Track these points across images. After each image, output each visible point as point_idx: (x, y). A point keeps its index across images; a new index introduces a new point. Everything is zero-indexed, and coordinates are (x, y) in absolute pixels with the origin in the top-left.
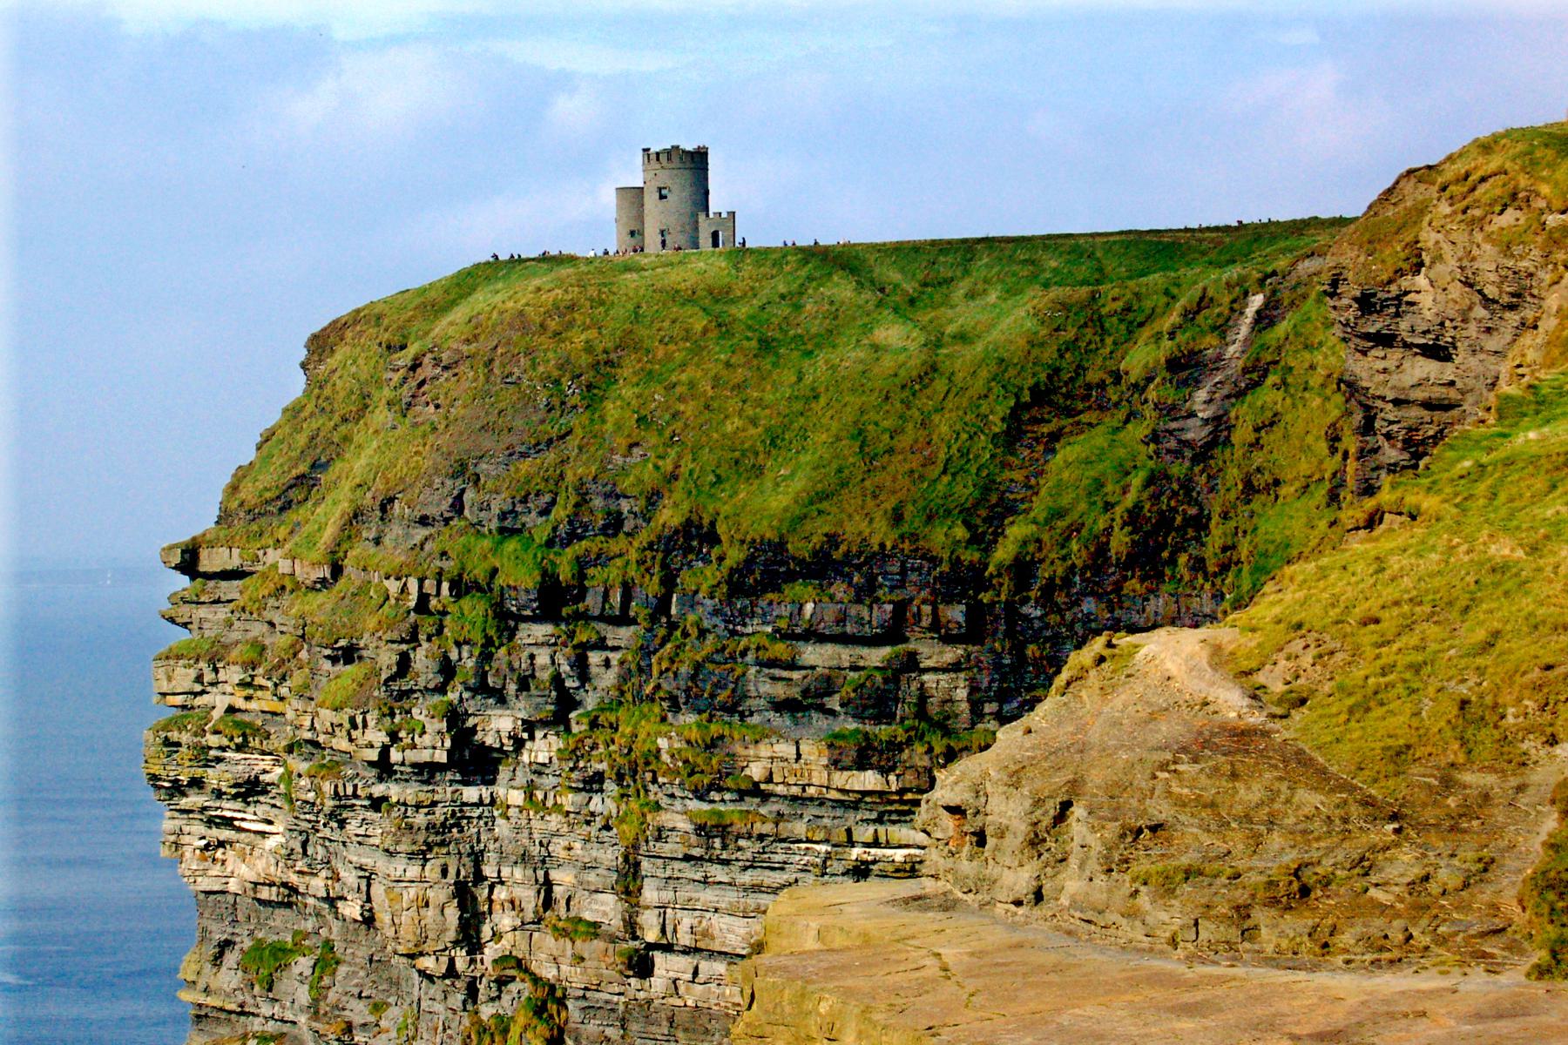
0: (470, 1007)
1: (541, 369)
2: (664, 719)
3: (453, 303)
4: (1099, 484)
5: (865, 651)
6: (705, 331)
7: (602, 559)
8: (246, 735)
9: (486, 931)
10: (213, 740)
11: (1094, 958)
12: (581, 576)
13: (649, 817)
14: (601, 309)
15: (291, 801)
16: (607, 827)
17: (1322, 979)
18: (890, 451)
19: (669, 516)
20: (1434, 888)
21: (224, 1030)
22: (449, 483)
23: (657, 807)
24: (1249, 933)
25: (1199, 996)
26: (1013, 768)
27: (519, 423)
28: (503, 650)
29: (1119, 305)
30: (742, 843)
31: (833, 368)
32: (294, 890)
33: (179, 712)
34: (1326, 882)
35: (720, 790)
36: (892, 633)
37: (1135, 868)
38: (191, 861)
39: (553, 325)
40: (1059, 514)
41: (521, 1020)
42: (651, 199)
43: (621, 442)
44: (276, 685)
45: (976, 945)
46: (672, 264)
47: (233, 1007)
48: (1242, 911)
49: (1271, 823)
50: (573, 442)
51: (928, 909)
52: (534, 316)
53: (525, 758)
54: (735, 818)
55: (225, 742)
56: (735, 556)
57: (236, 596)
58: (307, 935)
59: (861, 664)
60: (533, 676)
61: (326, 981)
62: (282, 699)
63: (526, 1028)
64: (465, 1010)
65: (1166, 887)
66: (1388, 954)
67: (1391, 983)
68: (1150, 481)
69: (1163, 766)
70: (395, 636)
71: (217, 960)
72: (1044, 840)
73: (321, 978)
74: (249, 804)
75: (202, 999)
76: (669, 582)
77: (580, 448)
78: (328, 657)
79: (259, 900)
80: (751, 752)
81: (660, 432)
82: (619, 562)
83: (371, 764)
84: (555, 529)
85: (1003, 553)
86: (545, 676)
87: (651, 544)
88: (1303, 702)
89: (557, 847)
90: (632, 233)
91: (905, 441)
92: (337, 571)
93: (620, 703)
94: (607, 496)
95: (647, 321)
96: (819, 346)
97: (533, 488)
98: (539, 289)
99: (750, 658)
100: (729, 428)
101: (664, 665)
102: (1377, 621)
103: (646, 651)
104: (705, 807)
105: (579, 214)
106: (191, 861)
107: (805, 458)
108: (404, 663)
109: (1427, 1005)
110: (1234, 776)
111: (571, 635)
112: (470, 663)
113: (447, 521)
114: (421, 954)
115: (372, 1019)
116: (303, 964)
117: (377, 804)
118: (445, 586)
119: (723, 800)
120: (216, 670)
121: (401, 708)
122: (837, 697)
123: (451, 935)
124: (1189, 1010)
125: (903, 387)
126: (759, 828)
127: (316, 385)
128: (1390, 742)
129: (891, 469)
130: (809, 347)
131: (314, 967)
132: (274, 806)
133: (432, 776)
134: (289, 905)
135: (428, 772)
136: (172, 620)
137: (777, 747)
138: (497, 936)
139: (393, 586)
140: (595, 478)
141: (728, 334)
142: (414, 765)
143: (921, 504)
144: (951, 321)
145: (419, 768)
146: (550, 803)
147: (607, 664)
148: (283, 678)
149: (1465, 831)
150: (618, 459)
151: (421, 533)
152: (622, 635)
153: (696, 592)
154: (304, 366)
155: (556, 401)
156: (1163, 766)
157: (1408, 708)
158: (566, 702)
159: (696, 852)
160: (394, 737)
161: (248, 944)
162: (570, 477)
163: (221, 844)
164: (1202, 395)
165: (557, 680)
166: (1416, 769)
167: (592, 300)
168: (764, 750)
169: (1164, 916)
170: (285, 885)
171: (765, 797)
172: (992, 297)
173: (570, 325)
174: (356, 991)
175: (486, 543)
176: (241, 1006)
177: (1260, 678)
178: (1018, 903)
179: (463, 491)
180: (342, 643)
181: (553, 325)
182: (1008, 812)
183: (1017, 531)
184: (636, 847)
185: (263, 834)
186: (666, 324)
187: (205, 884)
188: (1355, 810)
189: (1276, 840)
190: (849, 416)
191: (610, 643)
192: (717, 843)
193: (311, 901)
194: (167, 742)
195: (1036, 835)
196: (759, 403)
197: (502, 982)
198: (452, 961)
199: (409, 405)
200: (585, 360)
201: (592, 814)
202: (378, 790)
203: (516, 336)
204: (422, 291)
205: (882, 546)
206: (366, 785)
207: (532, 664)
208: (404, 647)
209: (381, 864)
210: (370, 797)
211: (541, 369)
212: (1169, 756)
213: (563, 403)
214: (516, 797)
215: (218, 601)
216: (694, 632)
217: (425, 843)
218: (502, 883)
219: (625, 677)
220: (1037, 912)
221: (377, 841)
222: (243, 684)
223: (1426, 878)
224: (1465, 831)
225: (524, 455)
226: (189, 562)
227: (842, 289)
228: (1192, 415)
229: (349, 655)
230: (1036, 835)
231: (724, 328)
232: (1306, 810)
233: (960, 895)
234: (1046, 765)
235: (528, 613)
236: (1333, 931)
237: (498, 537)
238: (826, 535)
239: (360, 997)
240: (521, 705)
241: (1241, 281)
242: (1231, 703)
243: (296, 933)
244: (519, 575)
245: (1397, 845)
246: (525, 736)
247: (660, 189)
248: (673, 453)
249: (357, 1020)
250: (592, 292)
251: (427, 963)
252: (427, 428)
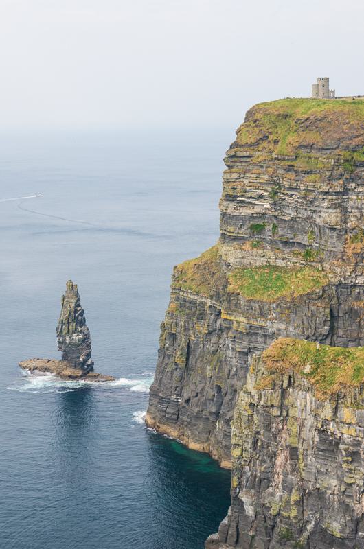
202: (325, 197)
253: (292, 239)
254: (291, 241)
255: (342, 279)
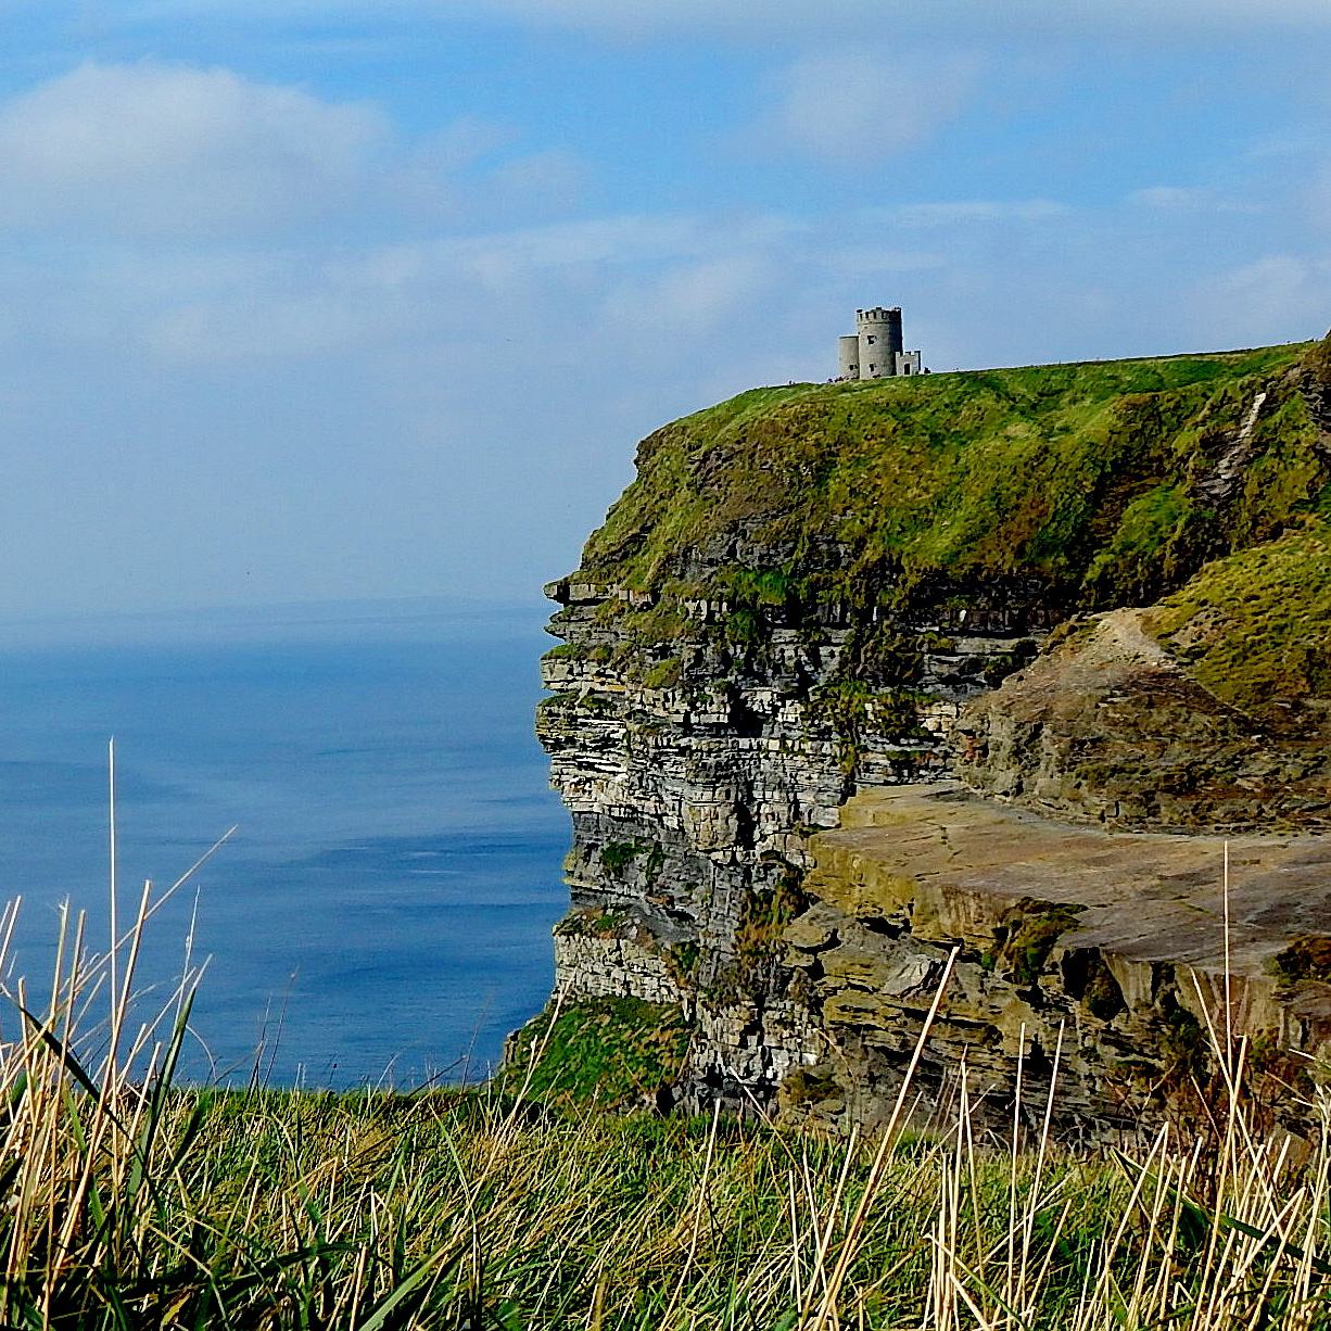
0: (746, 885)
1: (786, 459)
2: (869, 691)
3: (733, 417)
4: (1157, 525)
5: (1000, 642)
6: (895, 430)
7: (828, 585)
8: (601, 705)
9: (757, 835)
10: (580, 711)
11: (1051, 830)
12: (812, 596)
13: (861, 756)
14: (826, 418)
15: (630, 751)
16: (834, 764)
17: (1198, 840)
18: (1017, 507)
19: (870, 555)
20: (1282, 778)
21: (592, 903)
22: (726, 536)
23: (865, 750)
24: (1154, 812)
25: (1109, 852)
26: (1006, 703)
27: (771, 495)
28: (763, 647)
29: (1172, 404)
30: (922, 772)
31: (980, 453)
32: (635, 810)
33: (559, 694)
34: (1208, 775)
35: (907, 738)
36: (1019, 629)
37: (1079, 768)
38: (569, 792)
39: (793, 429)
40: (1131, 546)
41: (780, 893)
42: (863, 343)
43: (839, 506)
44: (619, 675)
45: (972, 822)
46: (873, 387)
47: (598, 888)
48: (1148, 796)
49: (1173, 737)
50: (807, 507)
51: (951, 800)
52: (781, 423)
53: (779, 719)
54: (917, 756)
55: (588, 713)
56: (913, 580)
57: (594, 616)
58: (644, 840)
59: (998, 650)
60: (783, 663)
61: (657, 870)
62: (623, 683)
63: (782, 900)
64: (743, 886)
65: (1099, 780)
66: (1243, 823)
67: (1244, 841)
68: (1187, 525)
69: (1104, 700)
70: (693, 639)
71: (587, 858)
72: (1024, 751)
73: (653, 868)
74: (604, 753)
75: (578, 883)
76: (871, 600)
77: (812, 510)
78: (649, 654)
79: (613, 817)
80: (927, 712)
81: (865, 499)
82: (839, 587)
83: (679, 724)
84: (796, 565)
85: (1092, 574)
86: (791, 663)
87: (859, 573)
88: (1201, 654)
89: (802, 779)
90: (851, 367)
91: (1025, 502)
92: (656, 597)
93: (841, 681)
94: (828, 542)
95: (856, 425)
96: (972, 438)
97: (783, 536)
98: (785, 406)
99: (925, 648)
100: (910, 495)
101: (869, 654)
102: (1257, 598)
103: (857, 643)
104: (898, 749)
105: (819, 356)
106: (569, 792)
107: (959, 514)
108: (699, 656)
109: (1262, 857)
110: (1151, 705)
111: (808, 636)
112: (742, 656)
113: (725, 562)
114: (715, 850)
115: (687, 894)
116: (642, 859)
117: (682, 751)
118: (725, 604)
119: (909, 745)
120: (582, 665)
121: (698, 687)
122: (983, 673)
123: (733, 837)
124: (1098, 862)
125: (1026, 464)
126: (933, 763)
127: (644, 475)
128: (1258, 680)
129: (1017, 519)
130: (964, 439)
131: (648, 861)
132: (620, 754)
133: (718, 732)
134: (632, 820)
135: (716, 729)
136: (553, 633)
137: (944, 708)
138: (763, 838)
139: (691, 606)
140: (822, 531)
141: (910, 433)
142: (705, 725)
143: (1036, 543)
144: (1059, 419)
145: (710, 726)
146: (796, 749)
147: (832, 655)
148: (623, 670)
149: (1308, 739)
150: (837, 517)
151: (709, 570)
152: (842, 635)
153: (890, 605)
154: (636, 462)
155: (795, 480)
156: (1104, 700)
157: (1273, 657)
158: (806, 681)
159: (893, 779)
160: (692, 704)
161: (606, 846)
162: (805, 531)
163: (588, 780)
164: (1224, 463)
165: (799, 666)
166: (1275, 698)
167: (819, 412)
168: (935, 710)
169: (1096, 800)
170: (629, 806)
171: (937, 741)
172: (1087, 402)
173: (806, 429)
174: (676, 876)
175: (751, 576)
176: (603, 886)
177: (1175, 639)
178: (1006, 794)
179: (735, 542)
180: (659, 645)
181: (793, 429)
182: (1001, 733)
183: (1102, 558)
184: (852, 775)
185: (614, 773)
186: (869, 426)
187: (577, 807)
188: (1231, 725)
189: (1177, 746)
190: (989, 485)
191: (834, 641)
192: (906, 772)
193: (646, 817)
194: (550, 714)
195: (1018, 747)
196: (931, 478)
197: (767, 868)
198: (734, 853)
199: (702, 486)
200: (814, 452)
201: (825, 755)
202: (683, 742)
203: (769, 437)
204: (713, 410)
205: (1011, 570)
206: (675, 739)
207: (783, 657)
208: (699, 646)
209: (686, 790)
210: (678, 746)
211: (786, 459)
212: (1108, 693)
213: (800, 481)
214: (775, 745)
215: (582, 620)
216: (888, 632)
217: (715, 776)
218: (766, 802)
219: (842, 664)
220: (1018, 800)
221: (683, 776)
222: (598, 674)
223: (1277, 771)
224: (1308, 739)
225: (775, 517)
226: (563, 594)
227: (987, 400)
228: (1219, 476)
229: (664, 652)
230: (1018, 747)
231: (908, 429)
232: (1197, 727)
233: (973, 790)
234: (1028, 700)
235: (779, 622)
236: (1210, 807)
237: (759, 572)
238: (973, 564)
239: (678, 880)
240: (776, 683)
241: (1251, 383)
242: (1154, 657)
243: (637, 838)
244: (773, 598)
245: (1259, 749)
246: (779, 704)
247: (869, 337)
248: (872, 512)
249: (677, 895)
250: (820, 407)
251: (717, 856)
252: (713, 500)
253: (680, 899)
254: (678, 907)
255: (720, 1060)
